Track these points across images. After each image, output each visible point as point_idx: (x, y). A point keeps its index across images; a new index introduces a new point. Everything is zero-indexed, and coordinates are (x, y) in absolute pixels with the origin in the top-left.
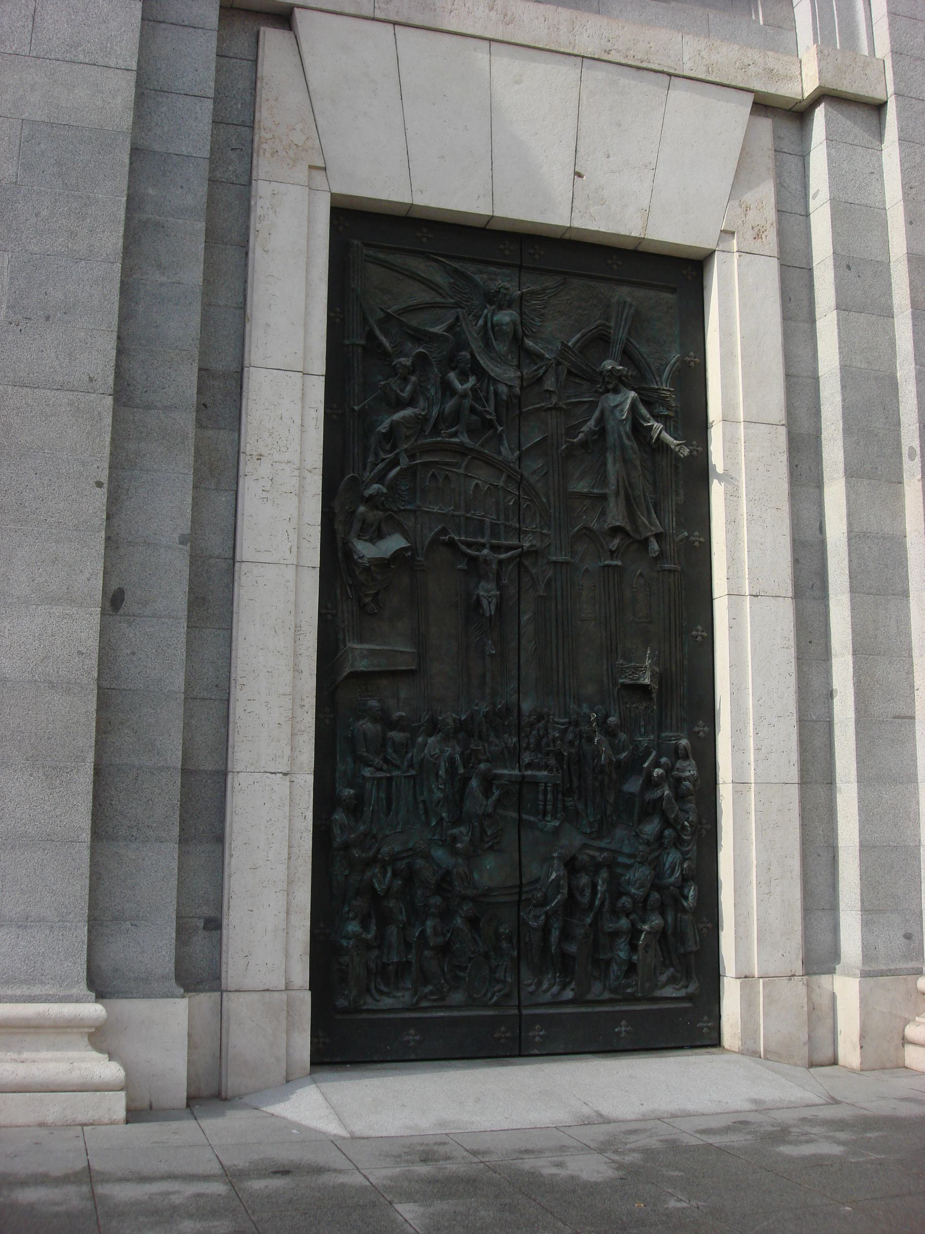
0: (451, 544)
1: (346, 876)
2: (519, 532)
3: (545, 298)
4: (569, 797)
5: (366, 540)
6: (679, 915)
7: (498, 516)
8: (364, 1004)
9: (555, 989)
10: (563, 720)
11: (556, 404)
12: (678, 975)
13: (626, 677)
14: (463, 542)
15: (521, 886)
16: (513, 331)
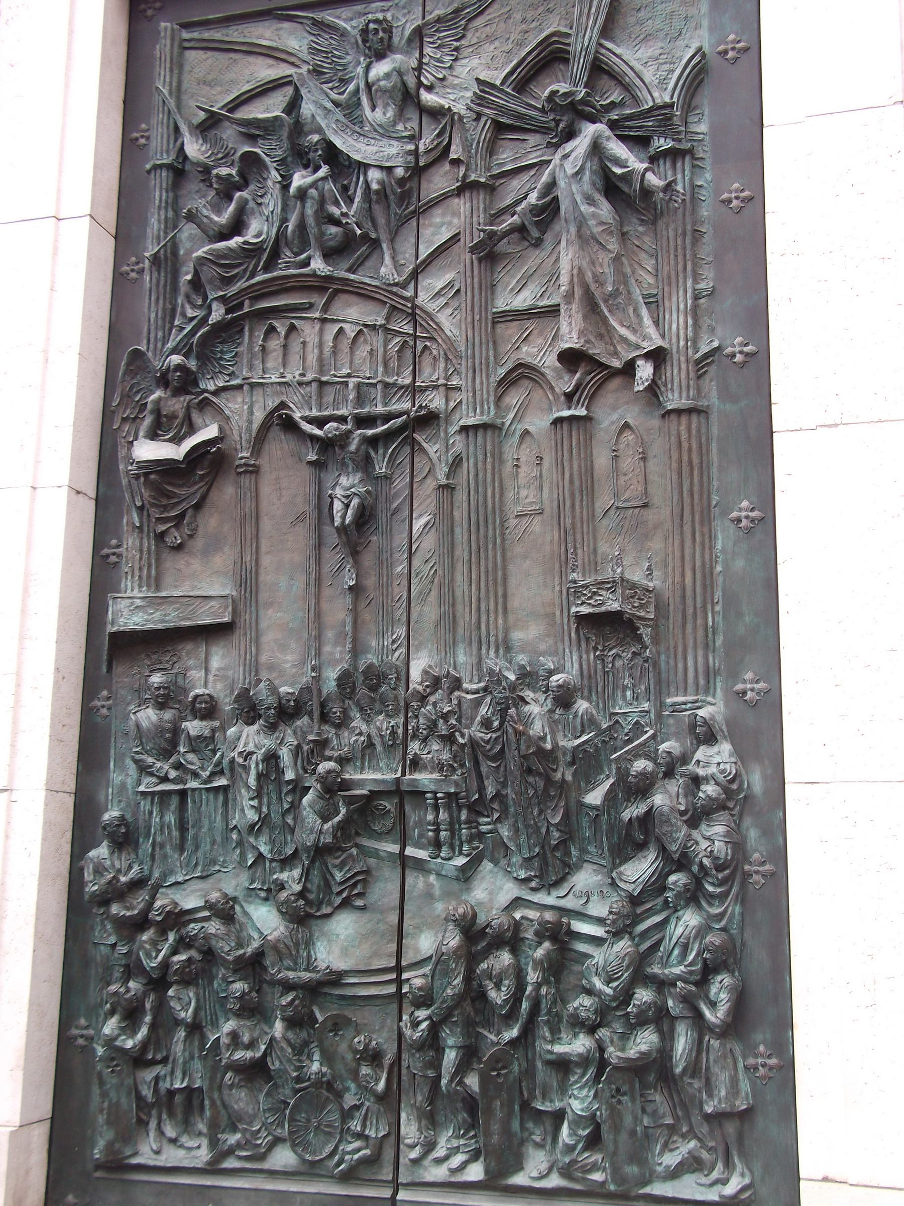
0: (289, 425)
1: (114, 946)
2: (414, 390)
3: (462, 22)
4: (488, 816)
5: (165, 441)
6: (707, 1038)
7: (376, 372)
8: (135, 1154)
9: (457, 1160)
10: (475, 686)
11: (465, 176)
12: (705, 1155)
13: (583, 603)
14: (311, 421)
15: (399, 968)
16: (399, 85)
